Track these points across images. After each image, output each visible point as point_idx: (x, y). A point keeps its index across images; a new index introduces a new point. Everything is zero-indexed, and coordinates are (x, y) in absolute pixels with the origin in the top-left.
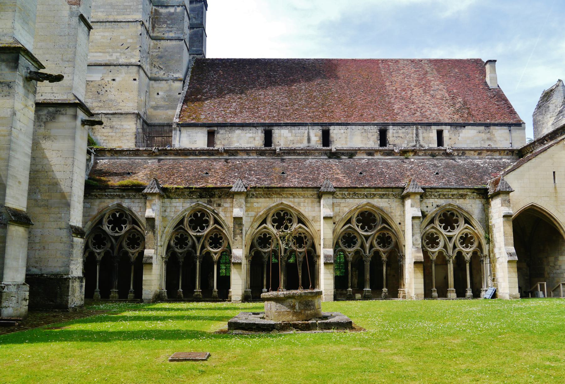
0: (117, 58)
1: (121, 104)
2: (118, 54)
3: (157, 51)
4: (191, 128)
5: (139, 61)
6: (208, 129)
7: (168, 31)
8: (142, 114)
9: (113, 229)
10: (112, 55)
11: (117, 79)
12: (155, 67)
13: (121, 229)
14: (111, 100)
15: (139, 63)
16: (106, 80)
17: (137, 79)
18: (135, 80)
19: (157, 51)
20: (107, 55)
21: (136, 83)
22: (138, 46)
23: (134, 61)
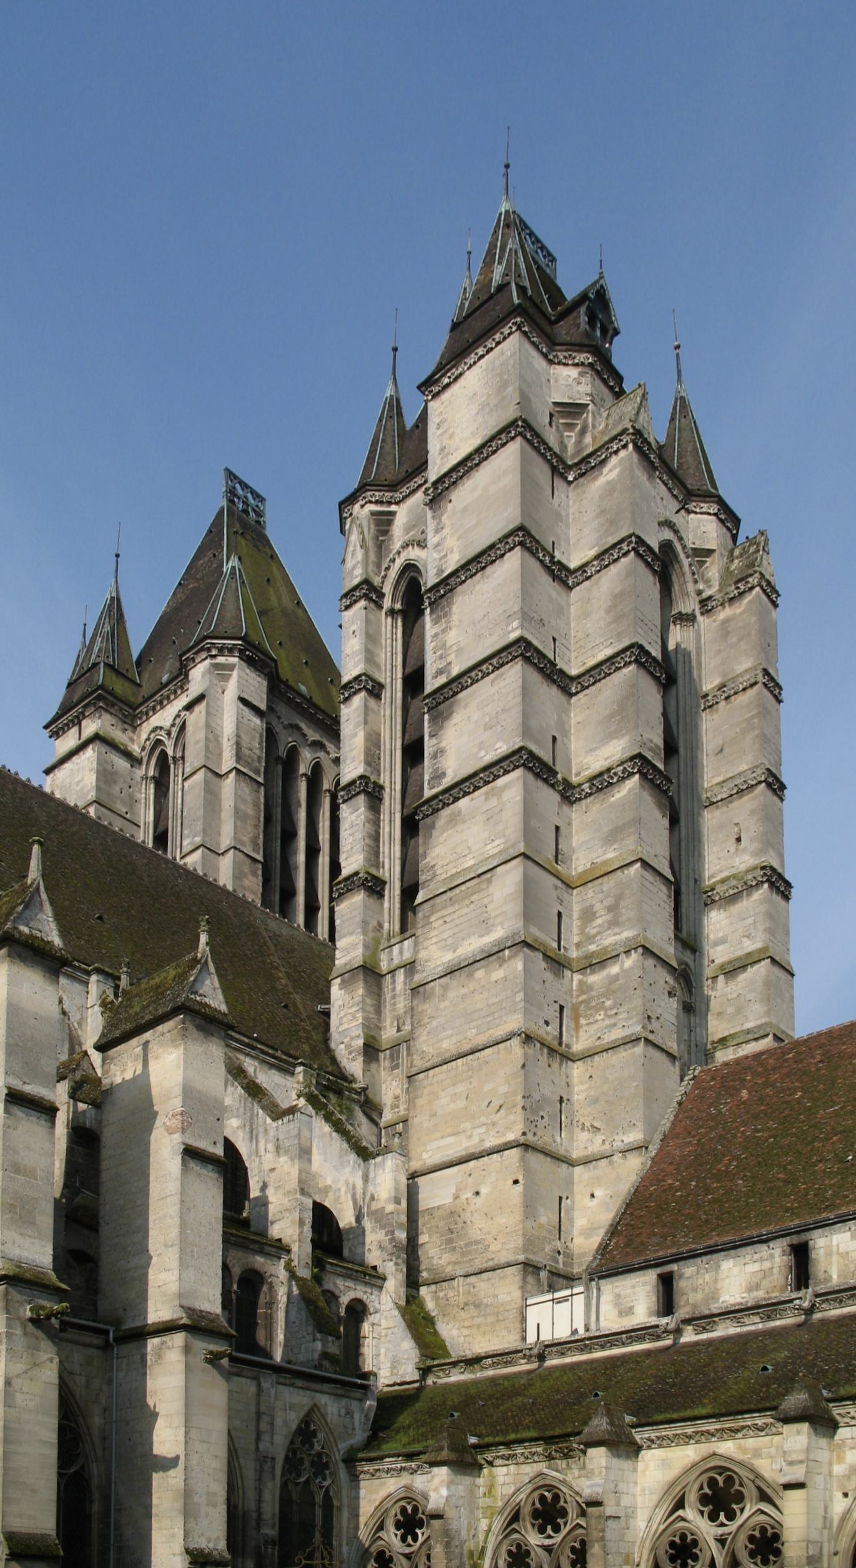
0: (482, 1141)
1: (492, 1248)
2: (483, 1130)
3: (585, 1086)
4: (621, 1277)
5: (524, 1134)
6: (659, 1270)
7: (607, 1027)
8: (539, 1259)
9: (404, 1539)
10: (471, 1136)
11: (484, 1191)
12: (583, 1129)
13: (415, 1539)
14: (477, 1242)
15: (522, 1140)
16: (463, 1197)
17: (521, 1179)
18: (516, 1182)
19: (585, 1086)
20: (462, 1137)
21: (519, 1188)
22: (519, 1098)
23: (511, 1137)
